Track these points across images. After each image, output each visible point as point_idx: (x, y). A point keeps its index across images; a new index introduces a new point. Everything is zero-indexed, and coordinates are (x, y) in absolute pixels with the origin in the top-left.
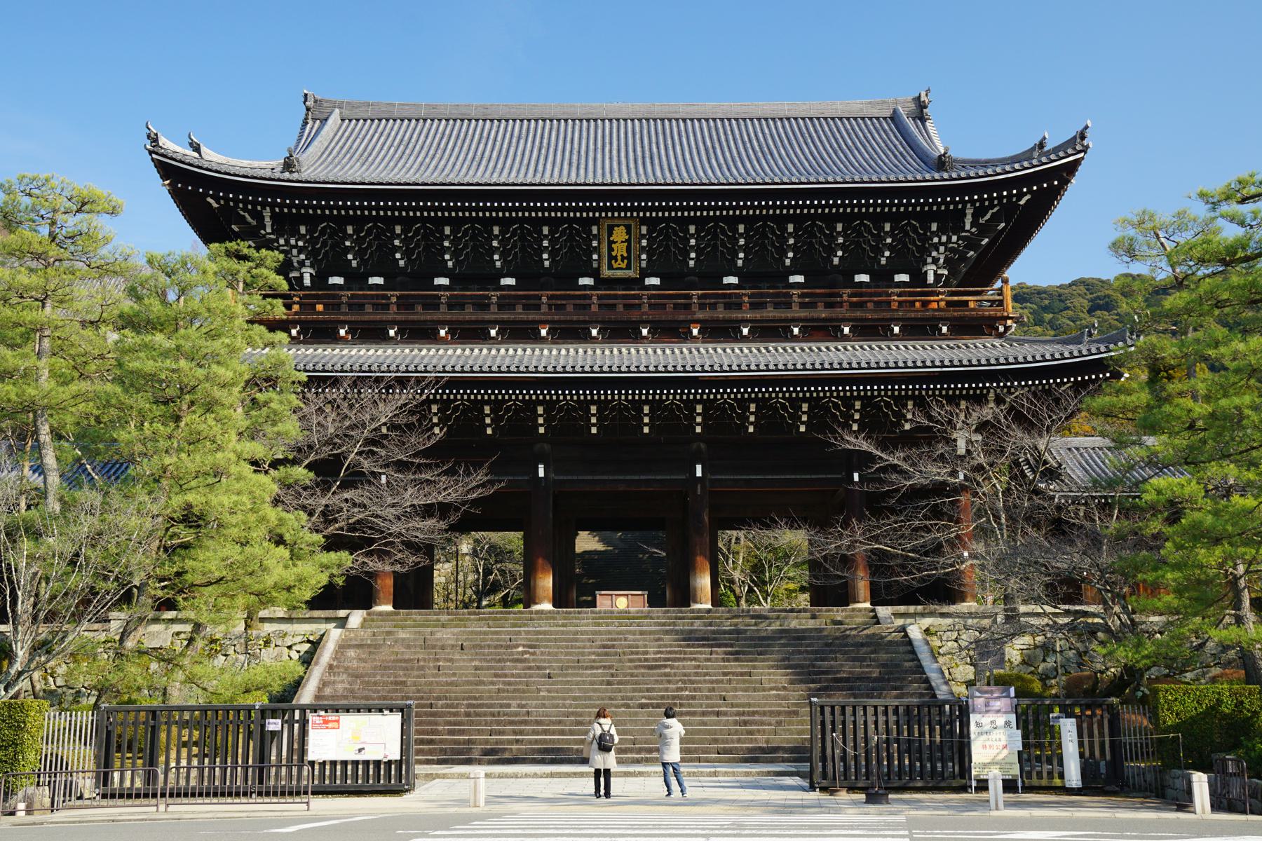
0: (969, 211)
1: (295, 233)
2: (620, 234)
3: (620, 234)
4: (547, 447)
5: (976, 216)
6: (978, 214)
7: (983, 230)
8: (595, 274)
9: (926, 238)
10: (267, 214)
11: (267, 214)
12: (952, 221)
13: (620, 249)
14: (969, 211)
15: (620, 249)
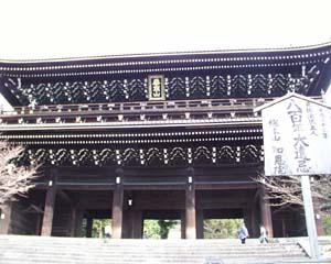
0: (304, 68)
1: (29, 87)
2: (156, 82)
3: (156, 82)
4: (121, 170)
5: (306, 71)
6: (308, 69)
7: (310, 76)
8: (147, 100)
9: (286, 81)
10: (19, 80)
11: (19, 80)
12: (296, 72)
13: (157, 89)
14: (304, 68)
15: (157, 89)
